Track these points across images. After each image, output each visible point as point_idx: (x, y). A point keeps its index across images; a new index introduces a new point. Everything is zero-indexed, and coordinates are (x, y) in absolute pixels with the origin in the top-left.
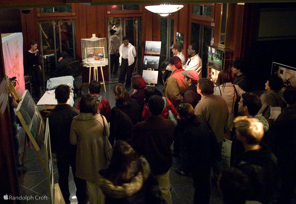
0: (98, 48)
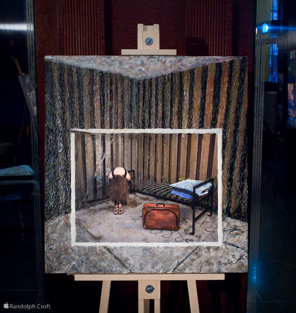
0: (177, 131)
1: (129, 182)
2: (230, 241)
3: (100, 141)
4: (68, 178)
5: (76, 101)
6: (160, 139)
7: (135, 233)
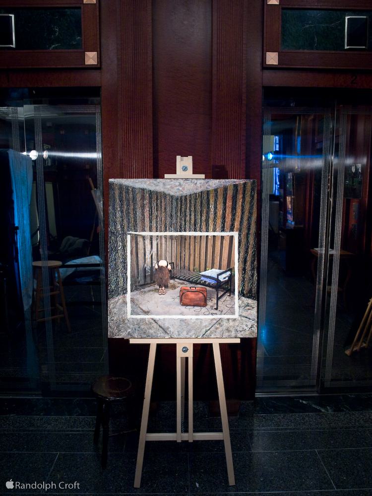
0: (205, 234)
1: (170, 271)
2: (244, 314)
3: (149, 241)
4: (125, 268)
5: (132, 212)
6: (192, 240)
7: (174, 308)
